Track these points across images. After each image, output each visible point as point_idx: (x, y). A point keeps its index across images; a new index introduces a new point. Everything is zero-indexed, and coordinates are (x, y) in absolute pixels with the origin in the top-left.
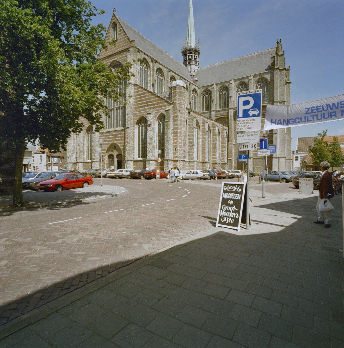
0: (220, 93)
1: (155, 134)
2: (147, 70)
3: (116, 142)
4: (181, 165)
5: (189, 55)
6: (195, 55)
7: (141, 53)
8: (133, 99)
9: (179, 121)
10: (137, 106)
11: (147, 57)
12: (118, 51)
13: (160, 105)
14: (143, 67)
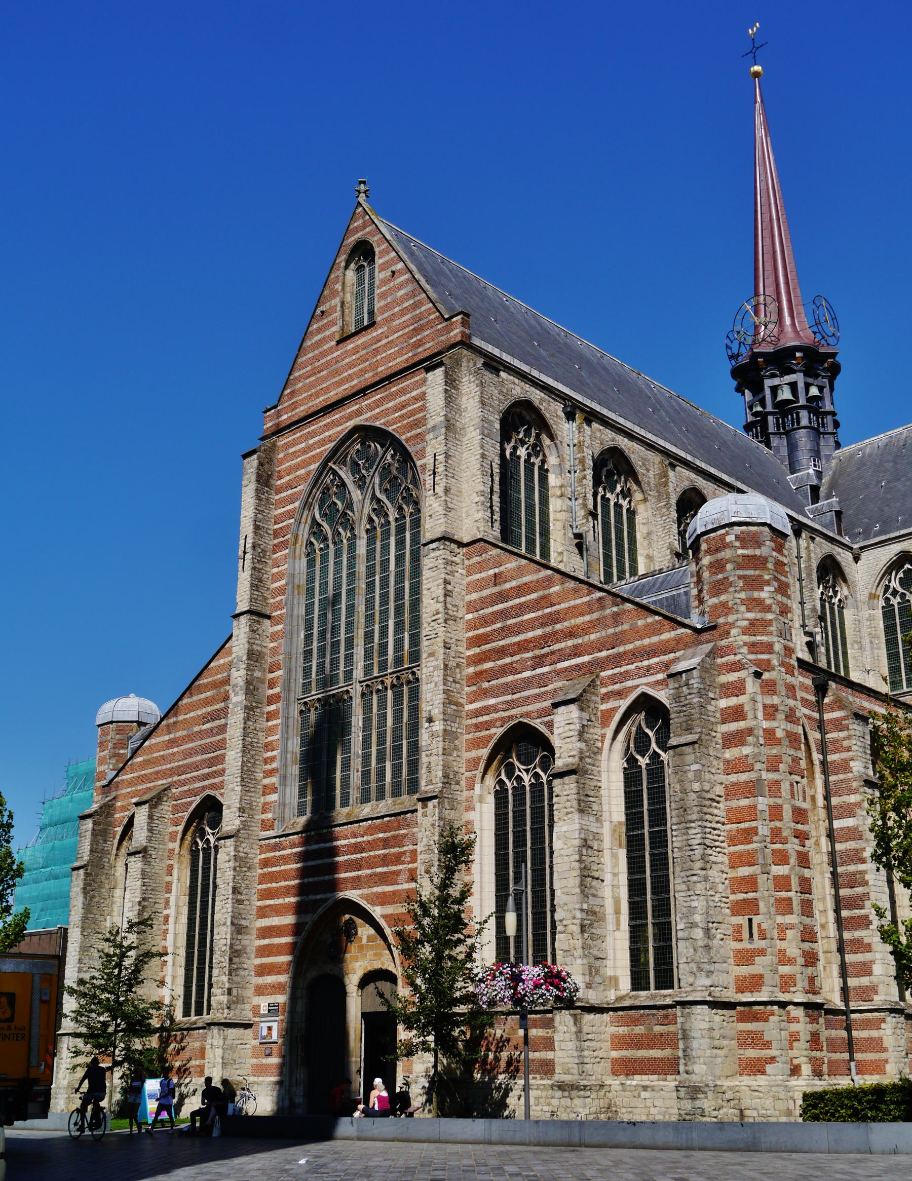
1: (606, 831)
2: (543, 462)
3: (358, 892)
4: (794, 1038)
5: (776, 381)
7: (502, 374)
8: (461, 625)
9: (762, 741)
11: (536, 396)
12: (377, 379)
13: (629, 647)
14: (515, 448)
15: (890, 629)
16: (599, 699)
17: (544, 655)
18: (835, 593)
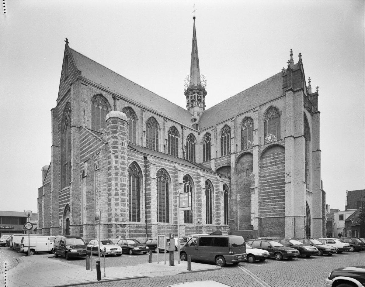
0: (222, 136)
6: (198, 95)
10: (82, 155)
15: (204, 149)
16: (94, 161)
17: (88, 152)
18: (193, 142)
